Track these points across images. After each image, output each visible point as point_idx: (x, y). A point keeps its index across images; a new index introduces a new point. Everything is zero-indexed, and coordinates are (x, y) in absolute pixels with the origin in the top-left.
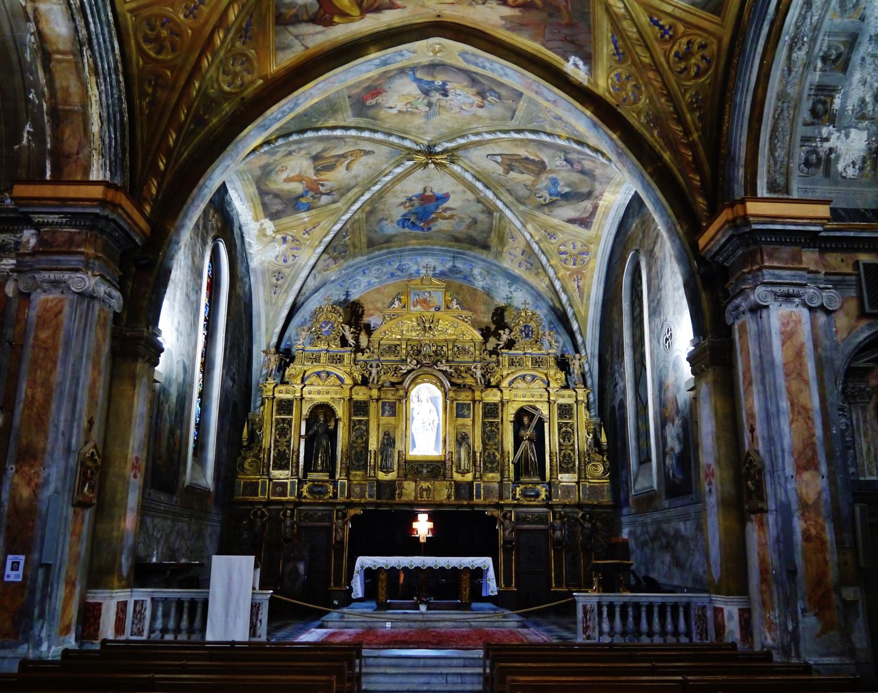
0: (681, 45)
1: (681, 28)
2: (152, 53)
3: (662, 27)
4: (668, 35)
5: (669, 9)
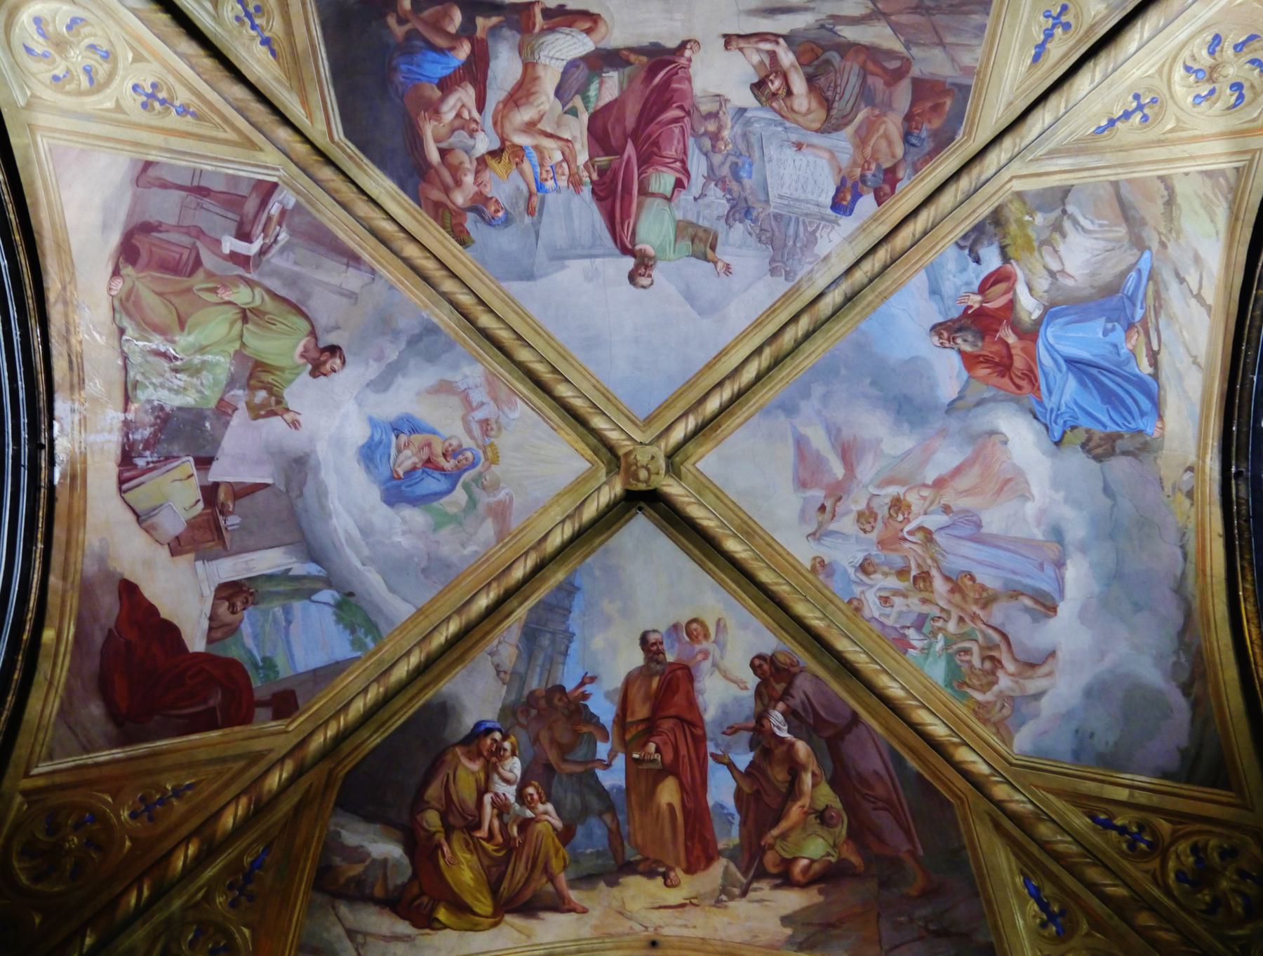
0: (1182, 856)
1: (1165, 826)
2: (24, 879)
3: (1122, 830)
4: (1144, 842)
5: (1123, 794)
